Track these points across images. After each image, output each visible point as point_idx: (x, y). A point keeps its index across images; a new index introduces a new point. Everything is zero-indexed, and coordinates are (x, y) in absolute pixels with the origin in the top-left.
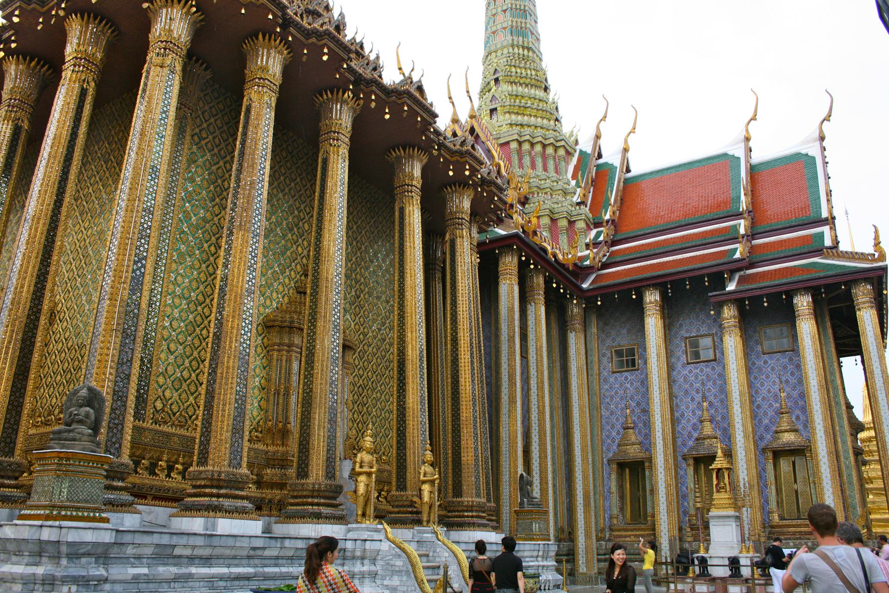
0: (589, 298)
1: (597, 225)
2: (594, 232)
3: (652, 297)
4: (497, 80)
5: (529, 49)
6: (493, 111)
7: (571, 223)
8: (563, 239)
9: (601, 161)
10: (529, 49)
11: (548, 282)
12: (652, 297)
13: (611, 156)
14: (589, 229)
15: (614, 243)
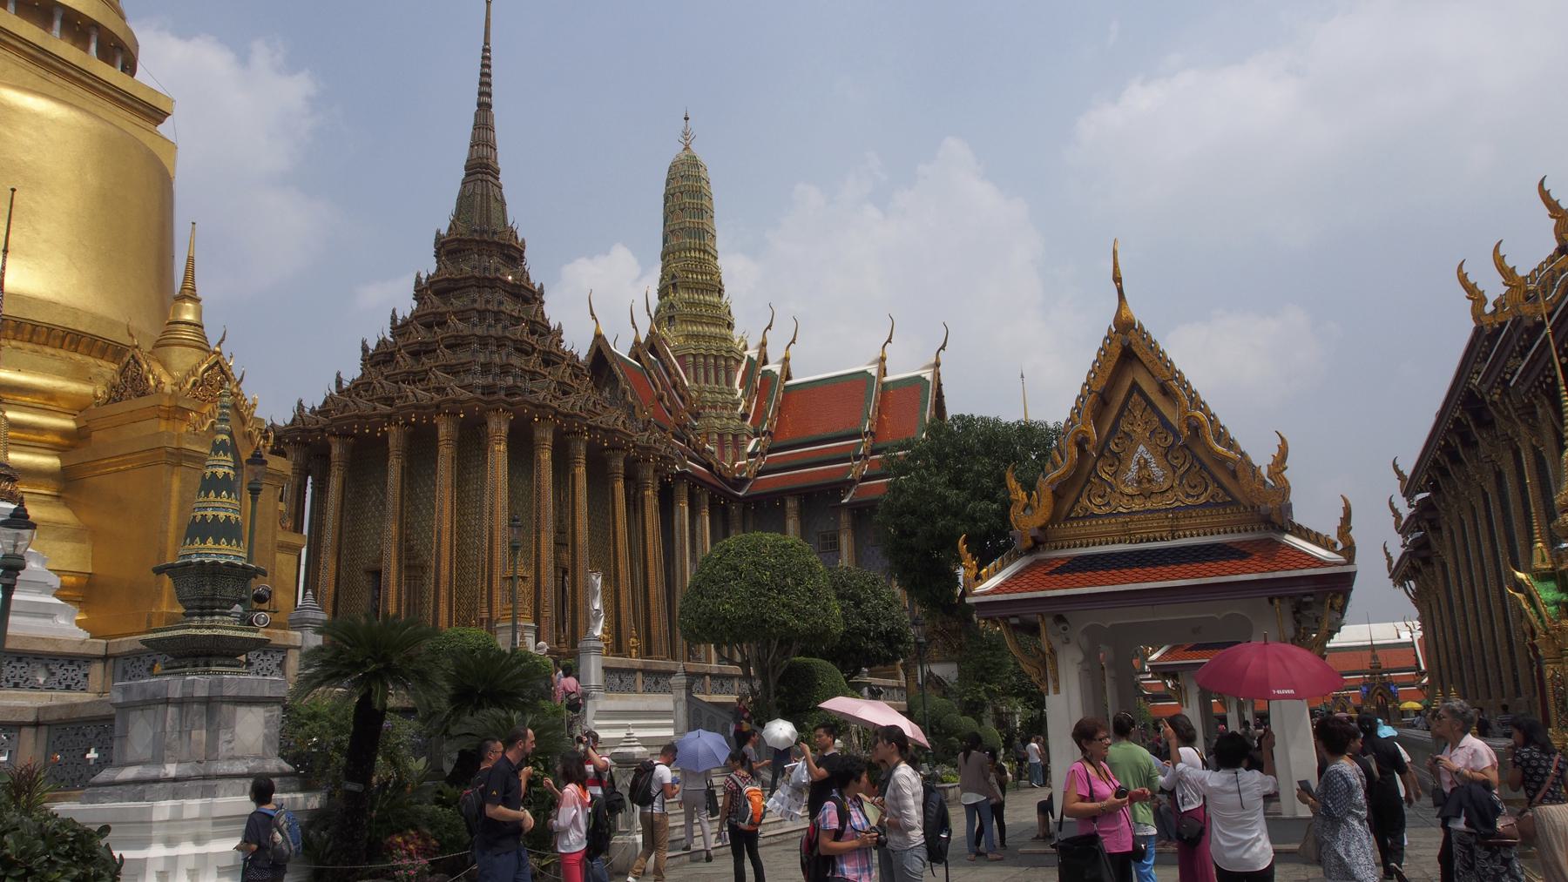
0: (745, 501)
1: (756, 435)
2: (754, 441)
3: (791, 504)
4: (674, 285)
5: (705, 251)
6: (671, 318)
7: (735, 436)
8: (730, 452)
9: (765, 368)
10: (705, 251)
11: (711, 498)
12: (791, 504)
13: (774, 367)
14: (750, 439)
15: (770, 451)
